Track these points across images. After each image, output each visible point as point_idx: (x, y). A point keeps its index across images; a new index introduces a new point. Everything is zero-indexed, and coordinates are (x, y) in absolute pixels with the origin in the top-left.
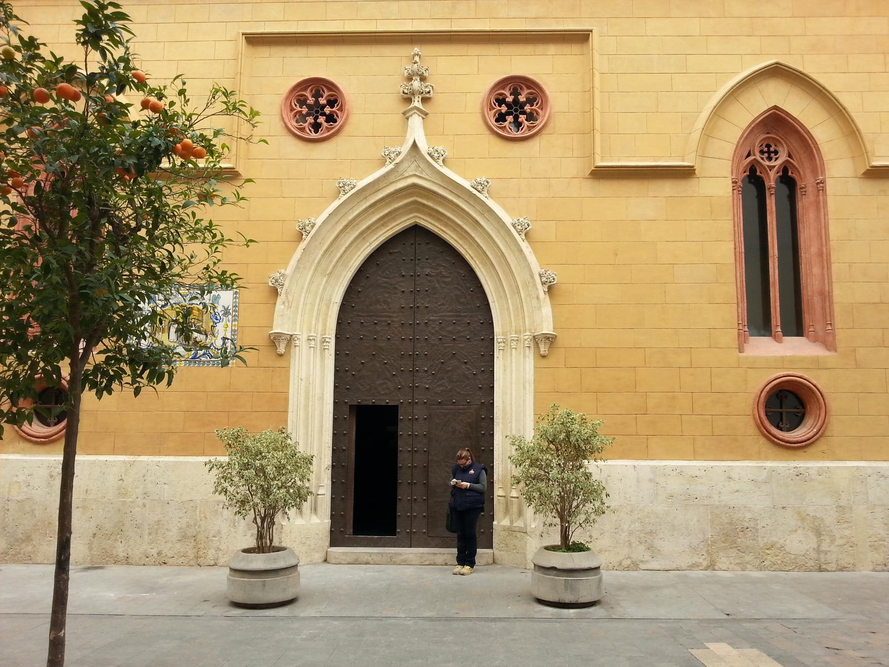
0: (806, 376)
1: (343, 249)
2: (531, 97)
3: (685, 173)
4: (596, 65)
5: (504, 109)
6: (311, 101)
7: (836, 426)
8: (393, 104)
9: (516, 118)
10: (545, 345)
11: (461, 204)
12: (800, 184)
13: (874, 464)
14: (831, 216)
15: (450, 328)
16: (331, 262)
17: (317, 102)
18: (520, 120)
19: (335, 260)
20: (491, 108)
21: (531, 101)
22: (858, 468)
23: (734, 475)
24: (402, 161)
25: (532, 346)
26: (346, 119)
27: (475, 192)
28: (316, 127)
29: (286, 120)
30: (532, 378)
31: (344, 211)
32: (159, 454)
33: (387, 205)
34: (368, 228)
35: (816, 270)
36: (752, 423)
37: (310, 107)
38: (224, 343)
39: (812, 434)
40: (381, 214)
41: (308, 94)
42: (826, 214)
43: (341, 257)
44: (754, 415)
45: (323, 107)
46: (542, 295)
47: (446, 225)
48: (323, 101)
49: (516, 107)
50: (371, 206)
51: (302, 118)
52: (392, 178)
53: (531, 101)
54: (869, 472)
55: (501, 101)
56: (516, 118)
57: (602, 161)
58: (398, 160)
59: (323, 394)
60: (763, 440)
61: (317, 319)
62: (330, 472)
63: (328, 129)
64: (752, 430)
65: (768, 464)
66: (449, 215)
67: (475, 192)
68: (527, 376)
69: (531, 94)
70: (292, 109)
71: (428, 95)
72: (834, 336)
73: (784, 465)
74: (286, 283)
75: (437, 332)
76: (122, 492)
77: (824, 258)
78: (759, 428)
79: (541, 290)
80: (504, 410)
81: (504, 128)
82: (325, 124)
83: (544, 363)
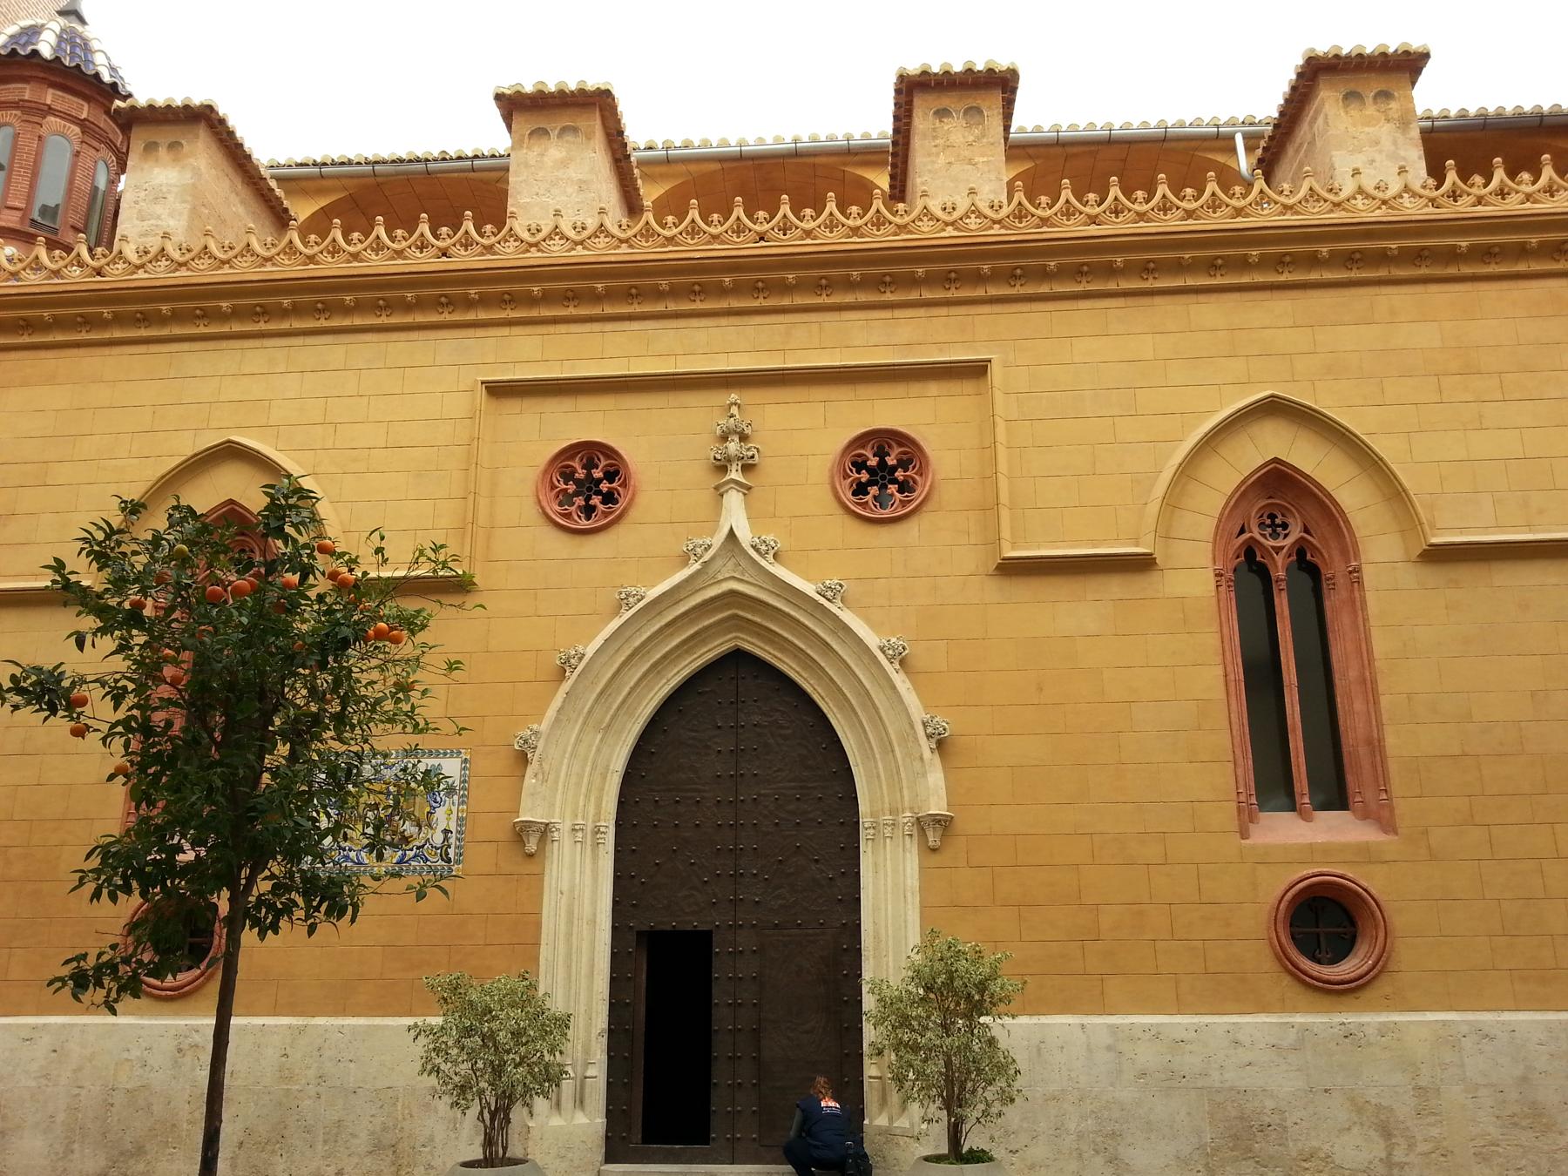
0: (1351, 875)
1: (627, 690)
3: (1141, 564)
4: (999, 410)
5: (864, 476)
6: (581, 474)
7: (1405, 954)
8: (698, 473)
10: (935, 832)
11: (802, 619)
12: (1326, 573)
13: (1470, 1016)
14: (1372, 622)
15: (791, 807)
17: (589, 475)
19: (615, 707)
20: (846, 476)
21: (904, 464)
22: (1444, 1023)
23: (1241, 1037)
24: (713, 558)
25: (915, 833)
26: (632, 499)
27: (822, 601)
28: (589, 511)
29: (544, 504)
30: (917, 884)
31: (628, 634)
32: (344, 1012)
33: (692, 622)
34: (665, 657)
35: (1358, 705)
36: (1268, 951)
37: (578, 482)
38: (446, 839)
39: (1365, 968)
41: (576, 464)
42: (1365, 620)
43: (624, 701)
44: (1270, 939)
45: (600, 481)
46: (927, 754)
47: (783, 650)
48: (597, 474)
49: (882, 473)
50: (668, 625)
51: (565, 498)
52: (699, 583)
53: (904, 464)
54: (1464, 1029)
55: (860, 465)
57: (1013, 549)
58: (707, 557)
59: (595, 915)
60: (1287, 980)
61: (587, 797)
62: (605, 1041)
63: (606, 515)
64: (1269, 963)
65: (1299, 1019)
66: (785, 634)
67: (822, 601)
68: (909, 882)
70: (553, 487)
72: (1392, 809)
73: (1323, 1020)
74: (541, 745)
76: (285, 1075)
77: (1369, 687)
78: (1279, 959)
79: (926, 746)
80: (876, 937)
81: (864, 505)
82: (601, 507)
83: (935, 860)
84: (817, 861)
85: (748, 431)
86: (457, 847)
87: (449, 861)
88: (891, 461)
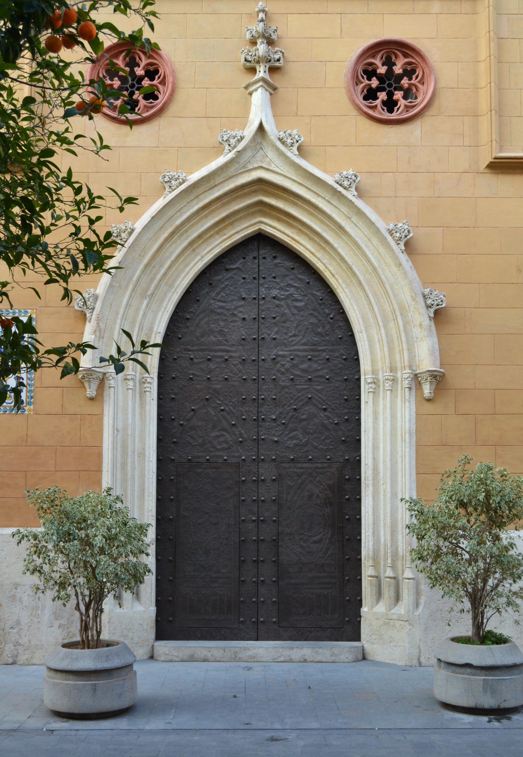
1: (169, 263)
2: (409, 68)
5: (375, 83)
9: (390, 95)
16: (153, 279)
18: (395, 97)
21: (409, 73)
34: (200, 236)
40: (217, 219)
43: (165, 274)
56: (390, 95)
59: (144, 449)
69: (410, 63)
71: (277, 64)
75: (287, 370)
84: (325, 410)
85: (274, 37)
88: (398, 70)
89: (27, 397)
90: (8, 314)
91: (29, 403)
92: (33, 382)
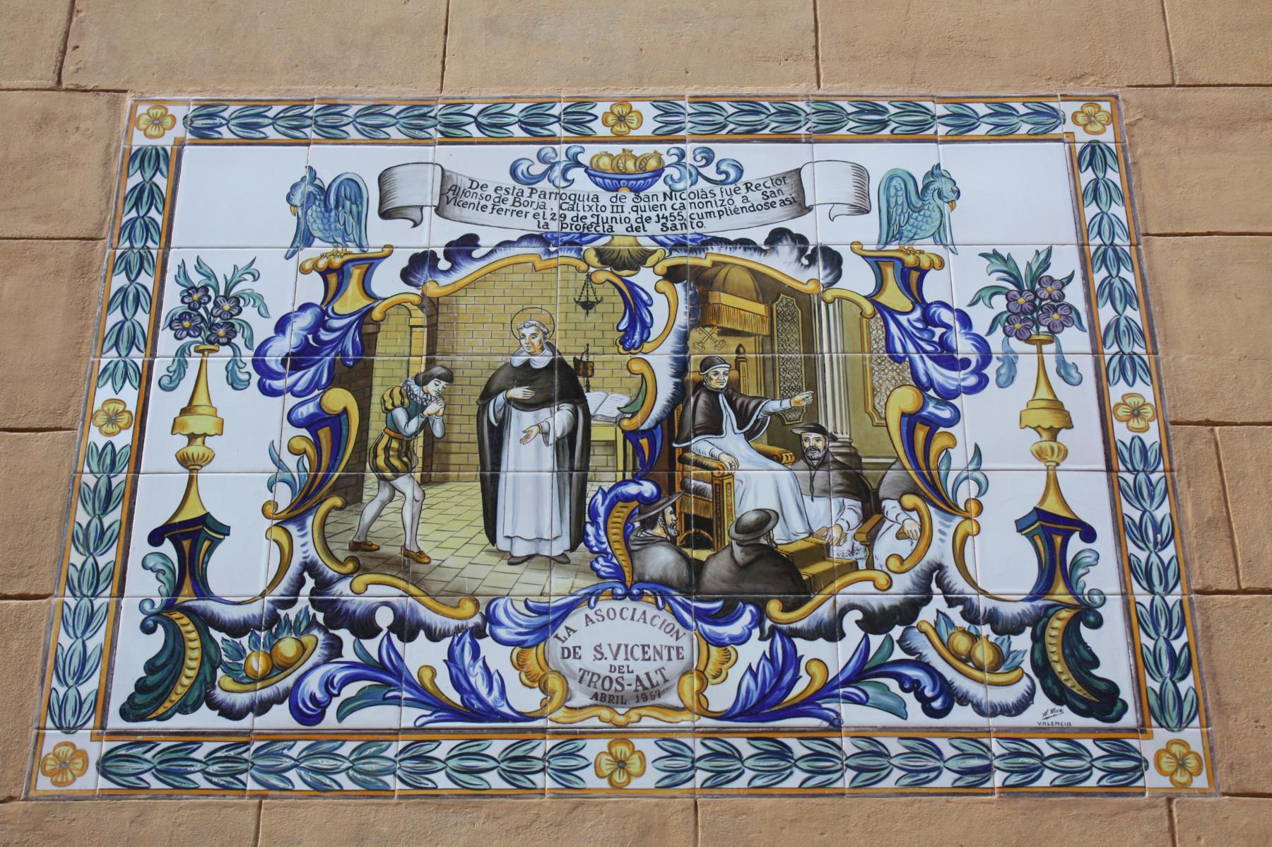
38: (1054, 568)
86: (1134, 620)
87: (1103, 701)
89: (1142, 663)
90: (923, 126)
91: (1160, 710)
92: (1168, 553)
